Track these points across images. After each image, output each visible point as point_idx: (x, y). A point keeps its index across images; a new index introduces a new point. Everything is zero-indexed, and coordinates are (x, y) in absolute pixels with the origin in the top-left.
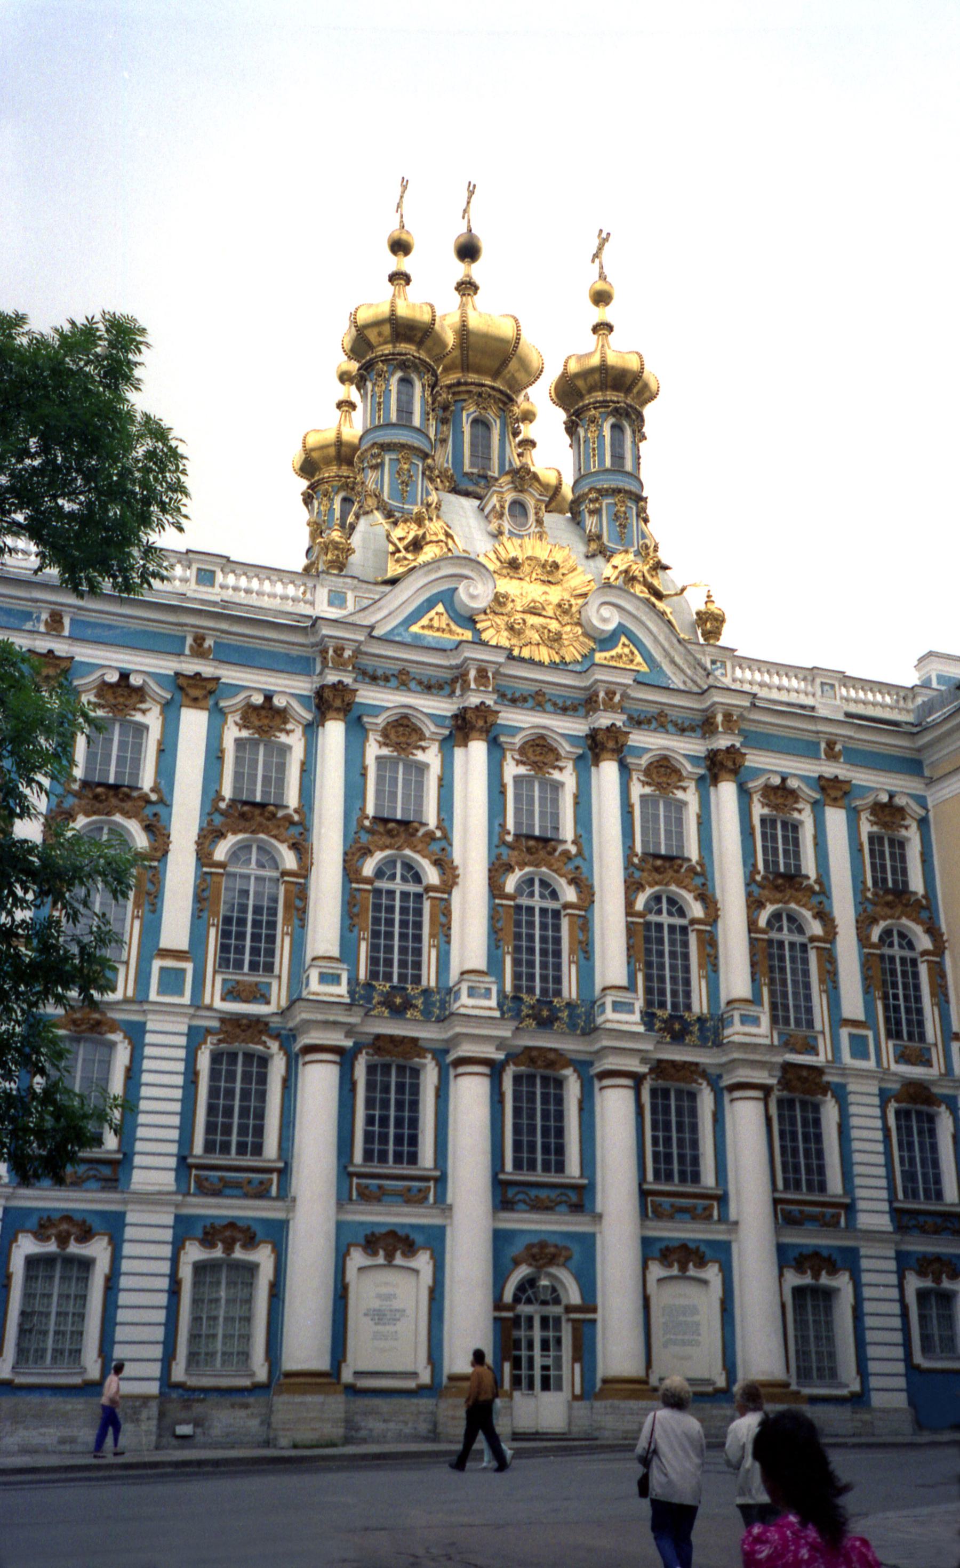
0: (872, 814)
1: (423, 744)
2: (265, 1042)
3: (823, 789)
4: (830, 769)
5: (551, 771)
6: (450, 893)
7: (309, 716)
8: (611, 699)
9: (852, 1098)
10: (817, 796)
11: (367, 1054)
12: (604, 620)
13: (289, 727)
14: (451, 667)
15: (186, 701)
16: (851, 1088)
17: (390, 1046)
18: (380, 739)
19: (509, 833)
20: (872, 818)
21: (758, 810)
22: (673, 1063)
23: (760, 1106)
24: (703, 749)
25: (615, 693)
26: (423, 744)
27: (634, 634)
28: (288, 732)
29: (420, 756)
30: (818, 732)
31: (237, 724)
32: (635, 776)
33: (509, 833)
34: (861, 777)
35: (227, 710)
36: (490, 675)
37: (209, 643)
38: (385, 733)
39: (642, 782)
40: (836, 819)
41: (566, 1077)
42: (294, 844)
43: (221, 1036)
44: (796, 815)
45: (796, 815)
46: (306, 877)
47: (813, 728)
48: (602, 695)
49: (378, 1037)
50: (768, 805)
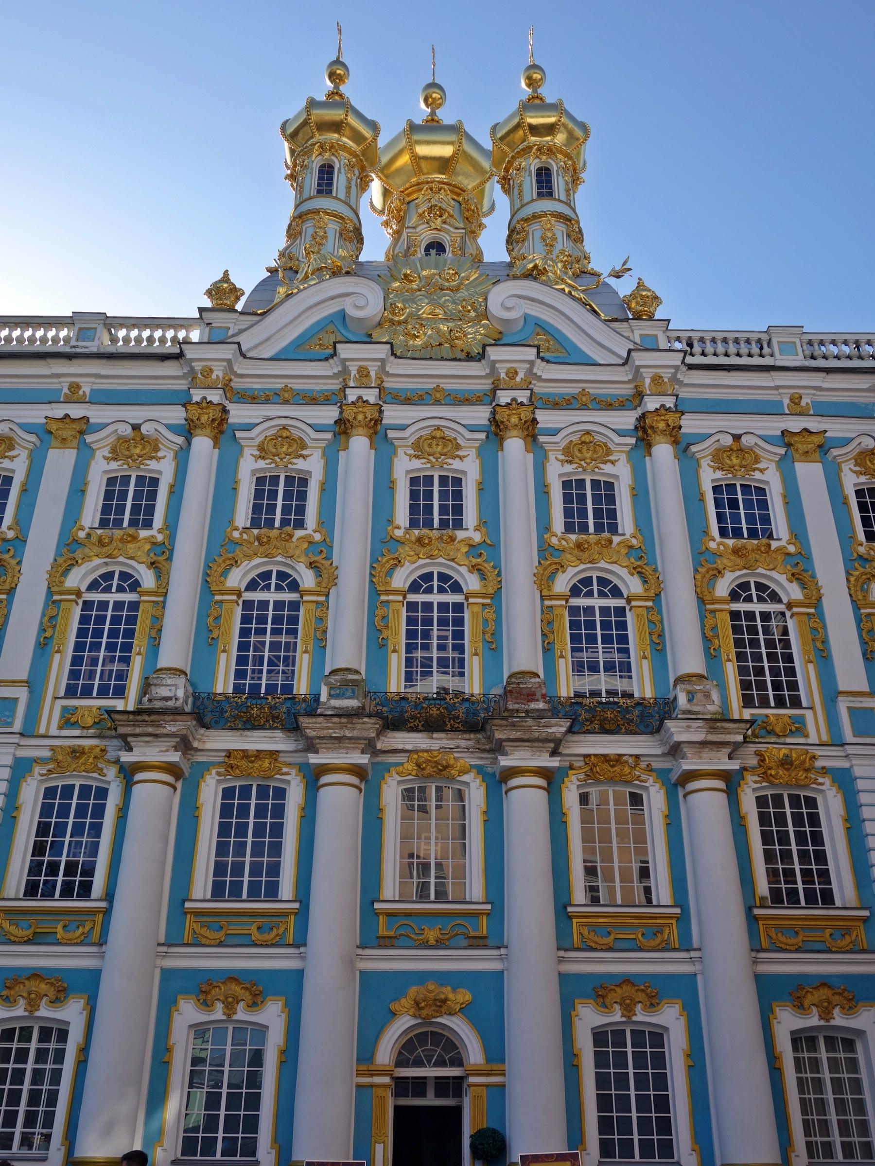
0: (856, 465)
1: (304, 452)
2: (102, 770)
3: (789, 445)
4: (795, 424)
5: (450, 461)
6: (327, 595)
7: (180, 440)
8: (513, 378)
9: (861, 784)
10: (782, 451)
11: (219, 774)
12: (508, 309)
13: (160, 454)
14: (335, 376)
15: (54, 443)
16: (858, 771)
17: (243, 763)
18: (258, 453)
19: (399, 528)
20: (857, 469)
21: (708, 477)
22: (605, 758)
23: (722, 798)
24: (633, 420)
25: (516, 373)
26: (304, 452)
27: (552, 326)
28: (158, 459)
29: (301, 464)
30: (777, 388)
31: (105, 458)
32: (552, 456)
33: (399, 528)
34: (836, 428)
35: (94, 446)
36: (373, 374)
37: (86, 389)
38: (261, 448)
39: (562, 461)
40: (810, 475)
41: (467, 784)
42: (152, 564)
43: (51, 766)
44: (757, 475)
45: (757, 475)
46: (165, 595)
47: (772, 384)
48: (503, 375)
49: (229, 754)
50: (722, 469)
